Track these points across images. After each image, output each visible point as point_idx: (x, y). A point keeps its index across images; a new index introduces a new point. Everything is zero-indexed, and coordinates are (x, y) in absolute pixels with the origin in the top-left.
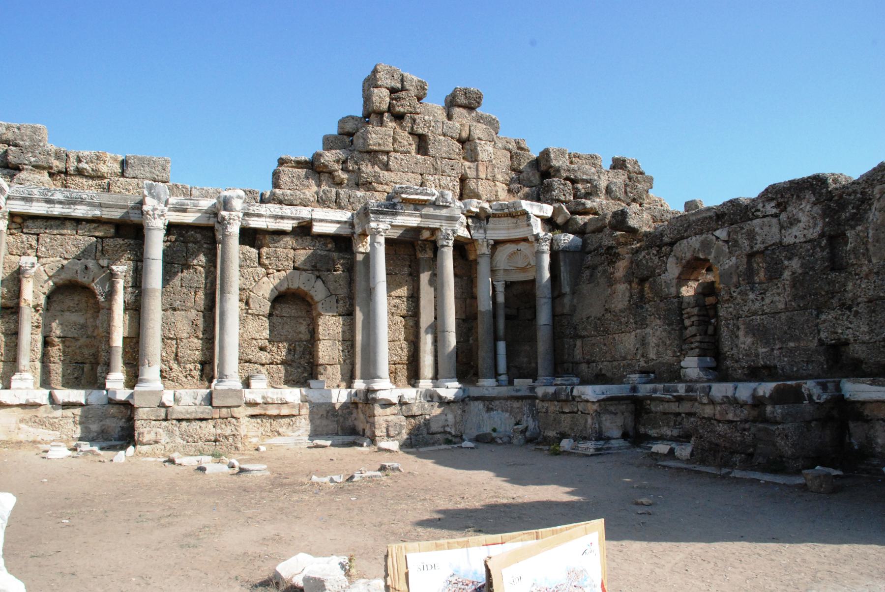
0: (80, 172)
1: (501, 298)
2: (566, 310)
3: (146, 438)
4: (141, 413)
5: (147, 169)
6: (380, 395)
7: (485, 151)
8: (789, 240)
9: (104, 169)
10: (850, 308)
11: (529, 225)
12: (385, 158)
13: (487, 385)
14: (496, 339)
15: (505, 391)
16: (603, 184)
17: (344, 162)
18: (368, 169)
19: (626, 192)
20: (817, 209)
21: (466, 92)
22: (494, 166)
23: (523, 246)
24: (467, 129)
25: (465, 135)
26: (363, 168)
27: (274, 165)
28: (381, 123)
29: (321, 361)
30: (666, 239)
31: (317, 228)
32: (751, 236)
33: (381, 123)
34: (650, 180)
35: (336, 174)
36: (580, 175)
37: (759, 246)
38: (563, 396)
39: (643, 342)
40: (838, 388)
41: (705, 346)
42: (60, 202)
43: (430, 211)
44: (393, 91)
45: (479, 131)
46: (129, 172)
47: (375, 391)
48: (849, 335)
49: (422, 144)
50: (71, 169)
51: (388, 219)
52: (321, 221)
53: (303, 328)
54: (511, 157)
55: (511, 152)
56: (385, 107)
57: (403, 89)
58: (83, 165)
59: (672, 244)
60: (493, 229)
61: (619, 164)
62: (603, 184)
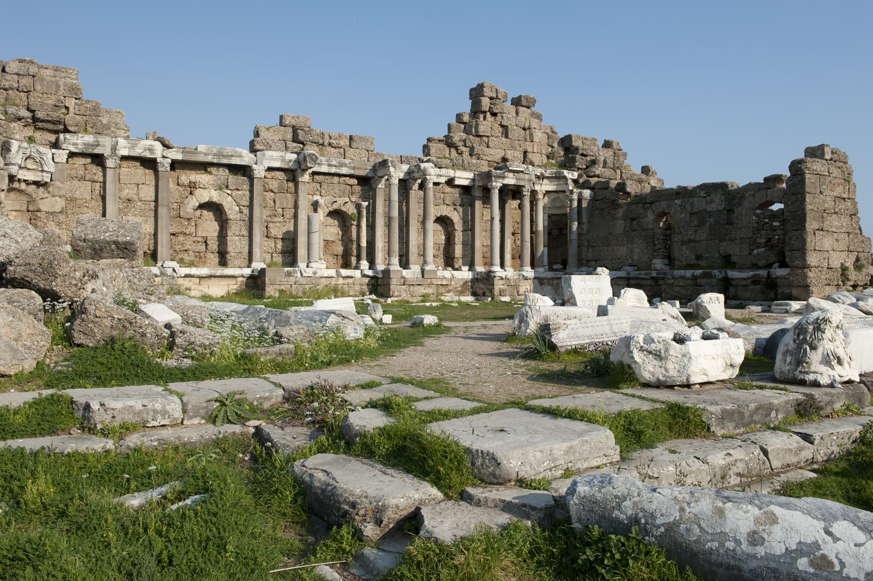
0: (330, 144)
3: (397, 294)
5: (363, 143)
7: (539, 136)
8: (709, 209)
9: (342, 143)
10: (733, 241)
11: (567, 184)
17: (464, 141)
20: (723, 197)
23: (561, 195)
24: (528, 122)
27: (425, 142)
29: (456, 256)
30: (647, 201)
32: (692, 205)
33: (485, 118)
34: (625, 155)
35: (459, 148)
36: (589, 152)
37: (695, 210)
39: (631, 251)
40: (726, 274)
41: (665, 254)
42: (335, 166)
43: (521, 174)
44: (491, 98)
45: (534, 123)
46: (354, 145)
47: (495, 272)
48: (731, 252)
50: (326, 143)
51: (501, 181)
52: (459, 178)
54: (548, 138)
56: (487, 109)
58: (331, 141)
59: (651, 203)
60: (546, 185)
61: (607, 145)
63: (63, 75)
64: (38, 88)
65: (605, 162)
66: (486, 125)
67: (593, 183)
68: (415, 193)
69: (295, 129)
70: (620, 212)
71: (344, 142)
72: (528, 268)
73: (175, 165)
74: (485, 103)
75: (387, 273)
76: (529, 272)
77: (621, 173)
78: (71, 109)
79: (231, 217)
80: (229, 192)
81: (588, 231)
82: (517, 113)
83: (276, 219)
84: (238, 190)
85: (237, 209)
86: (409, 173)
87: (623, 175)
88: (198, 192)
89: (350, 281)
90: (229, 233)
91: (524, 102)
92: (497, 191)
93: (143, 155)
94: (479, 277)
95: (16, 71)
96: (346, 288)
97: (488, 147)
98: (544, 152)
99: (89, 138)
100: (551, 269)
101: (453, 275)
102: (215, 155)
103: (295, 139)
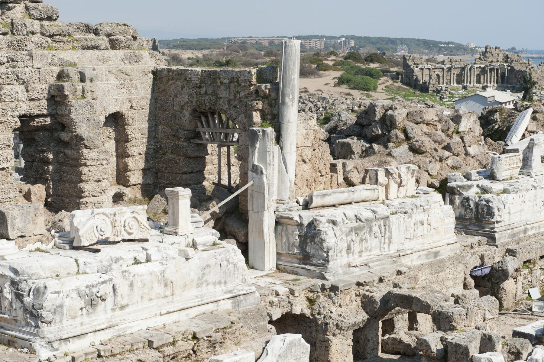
7: (500, 55)
13: (499, 84)
18: (486, 59)
49: (492, 55)
62: (515, 60)
66: (487, 55)
68: (472, 70)
71: (459, 61)
73: (433, 69)
74: (488, 50)
75: (467, 85)
76: (495, 85)
100: (502, 84)
103: (451, 61)
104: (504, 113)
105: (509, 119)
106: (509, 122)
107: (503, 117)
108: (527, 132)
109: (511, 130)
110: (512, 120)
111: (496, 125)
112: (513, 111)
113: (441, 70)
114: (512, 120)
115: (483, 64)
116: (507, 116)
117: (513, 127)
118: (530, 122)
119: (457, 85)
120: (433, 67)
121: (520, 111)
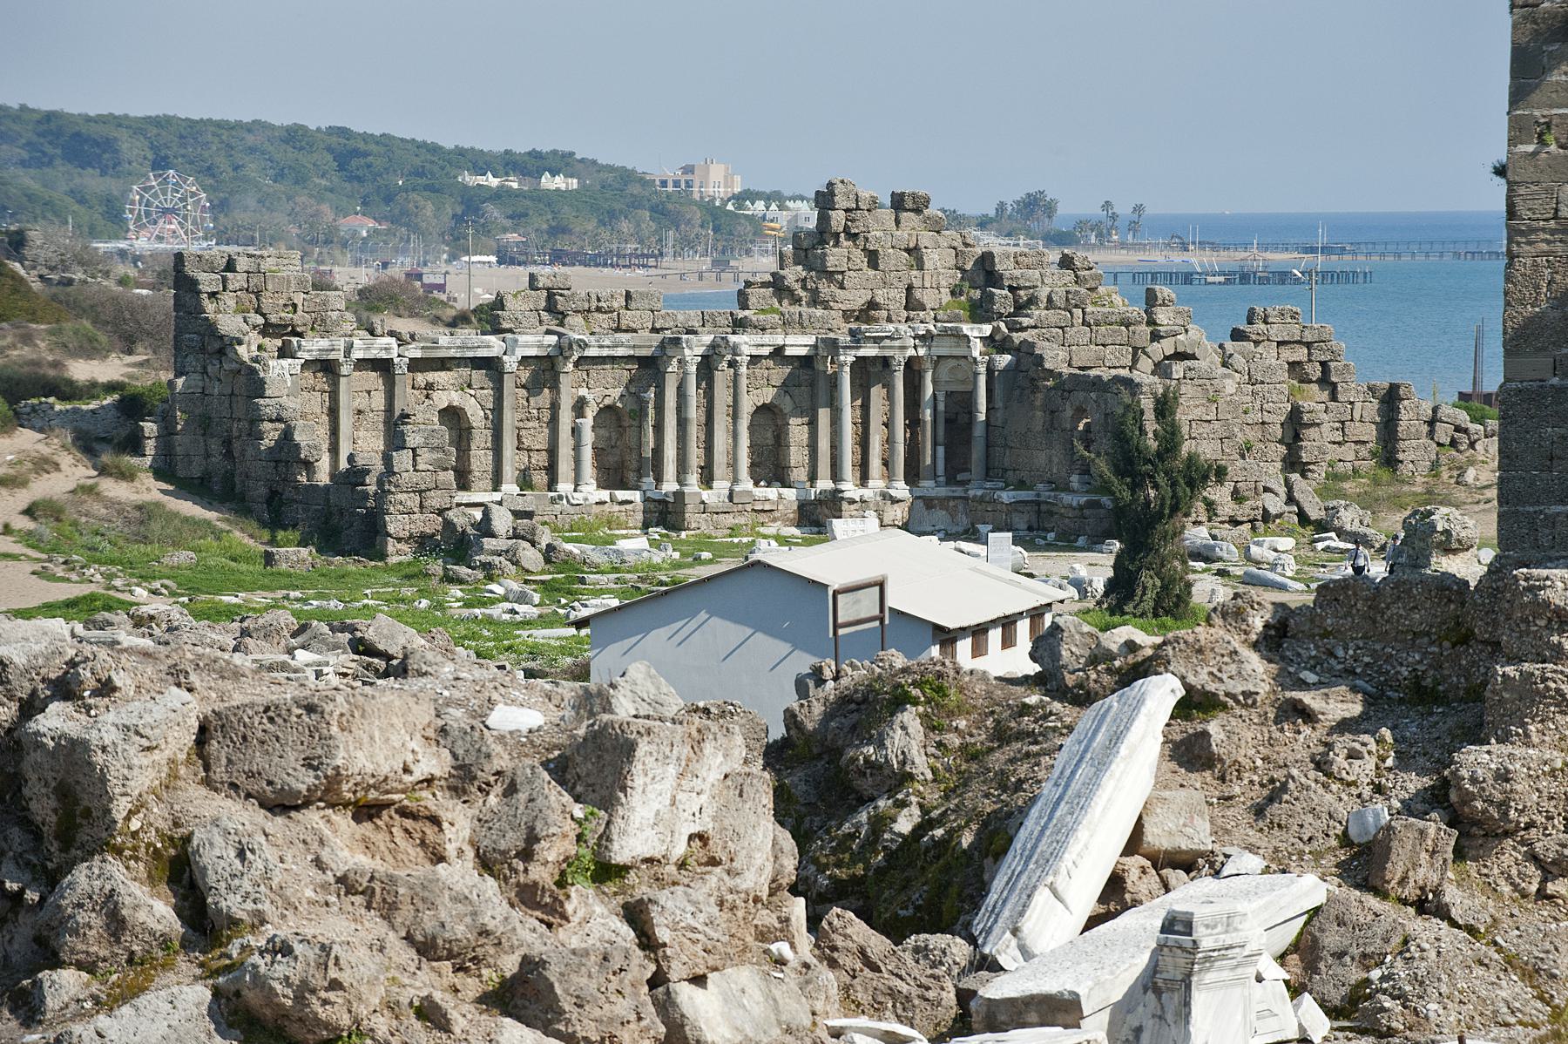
0: (598, 309)
1: (941, 407)
2: (999, 423)
4: (689, 508)
6: (846, 495)
7: (932, 258)
9: (616, 305)
12: (840, 277)
14: (935, 444)
15: (943, 492)
16: (1043, 293)
17: (804, 280)
18: (825, 289)
19: (1067, 299)
21: (914, 196)
22: (939, 274)
23: (962, 362)
25: (912, 245)
26: (820, 286)
28: (837, 244)
31: (789, 352)
33: (837, 244)
36: (1022, 283)
38: (987, 499)
43: (887, 342)
44: (847, 210)
46: (633, 305)
49: (873, 259)
51: (853, 352)
53: (769, 435)
55: (955, 248)
57: (858, 208)
58: (600, 304)
59: (1070, 392)
62: (1043, 293)
63: (286, 261)
64: (270, 287)
65: (1050, 299)
66: (835, 257)
67: (1017, 342)
68: (722, 377)
69: (550, 297)
70: (1039, 398)
71: (619, 302)
72: (901, 484)
74: (838, 219)
75: (679, 495)
76: (901, 489)
77: (1084, 313)
78: (300, 307)
79: (474, 424)
80: (472, 392)
81: (1005, 422)
82: (897, 222)
83: (531, 424)
84: (482, 388)
85: (482, 413)
86: (713, 346)
87: (1087, 318)
88: (435, 395)
89: (629, 507)
90: (473, 447)
91: (909, 204)
92: (847, 369)
93: (378, 356)
94: (822, 497)
95: (246, 268)
96: (623, 517)
97: (842, 287)
98: (944, 283)
99: (324, 343)
100: (951, 480)
101: (780, 495)
102: (459, 347)
103: (551, 307)
104: (960, 710)
105: (998, 759)
106: (1004, 788)
107: (954, 740)
108: (1138, 861)
109: (1017, 845)
110: (1023, 770)
111: (903, 804)
112: (1033, 699)
113: (478, 376)
114: (1023, 770)
115: (802, 326)
116: (980, 737)
117: (1031, 824)
118: (1161, 784)
119: (604, 495)
120: (414, 352)
121: (1083, 698)
